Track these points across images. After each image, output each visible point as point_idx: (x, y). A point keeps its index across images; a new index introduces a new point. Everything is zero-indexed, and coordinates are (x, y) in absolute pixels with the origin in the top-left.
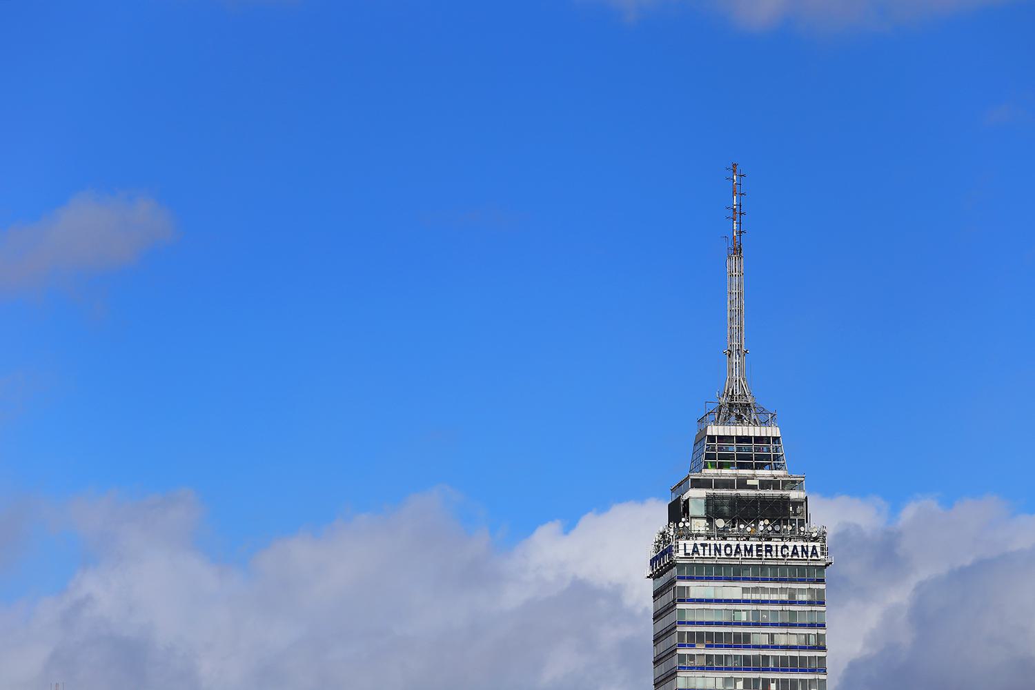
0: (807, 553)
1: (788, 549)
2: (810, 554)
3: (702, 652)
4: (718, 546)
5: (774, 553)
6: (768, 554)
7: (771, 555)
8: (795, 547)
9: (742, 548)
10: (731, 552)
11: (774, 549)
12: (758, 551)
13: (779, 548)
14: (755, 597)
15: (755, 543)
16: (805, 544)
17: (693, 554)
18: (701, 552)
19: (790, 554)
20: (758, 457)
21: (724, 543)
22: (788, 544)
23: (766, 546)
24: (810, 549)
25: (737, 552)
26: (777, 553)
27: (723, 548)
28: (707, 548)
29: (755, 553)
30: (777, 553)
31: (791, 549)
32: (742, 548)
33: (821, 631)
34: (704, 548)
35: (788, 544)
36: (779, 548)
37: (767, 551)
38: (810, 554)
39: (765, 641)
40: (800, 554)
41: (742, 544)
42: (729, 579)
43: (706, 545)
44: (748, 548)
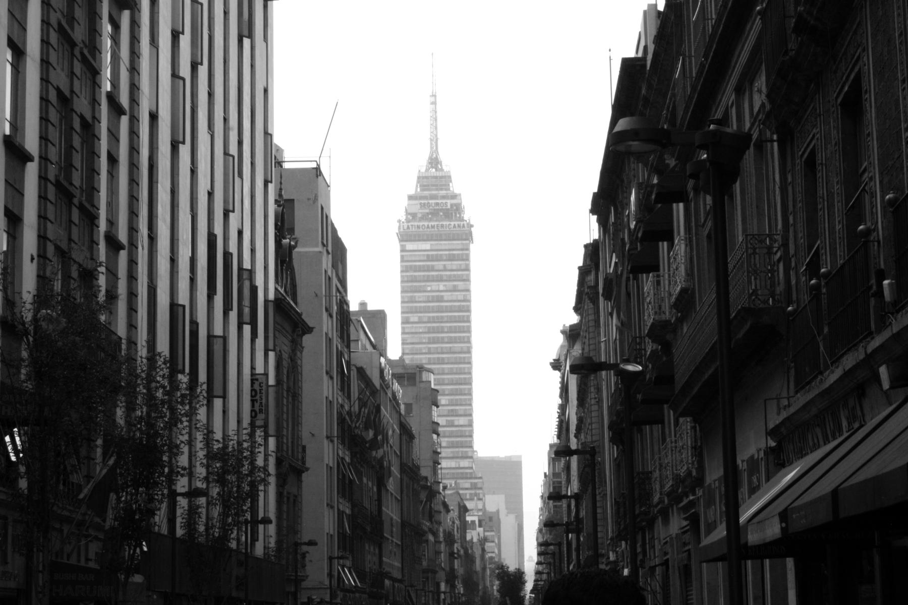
3: (412, 274)
8: (455, 225)
9: (430, 226)
14: (436, 248)
15: (436, 223)
16: (459, 223)
20: (441, 185)
21: (421, 224)
24: (462, 225)
31: (452, 226)
32: (430, 226)
33: (467, 262)
39: (441, 267)
41: (430, 224)
42: (424, 240)
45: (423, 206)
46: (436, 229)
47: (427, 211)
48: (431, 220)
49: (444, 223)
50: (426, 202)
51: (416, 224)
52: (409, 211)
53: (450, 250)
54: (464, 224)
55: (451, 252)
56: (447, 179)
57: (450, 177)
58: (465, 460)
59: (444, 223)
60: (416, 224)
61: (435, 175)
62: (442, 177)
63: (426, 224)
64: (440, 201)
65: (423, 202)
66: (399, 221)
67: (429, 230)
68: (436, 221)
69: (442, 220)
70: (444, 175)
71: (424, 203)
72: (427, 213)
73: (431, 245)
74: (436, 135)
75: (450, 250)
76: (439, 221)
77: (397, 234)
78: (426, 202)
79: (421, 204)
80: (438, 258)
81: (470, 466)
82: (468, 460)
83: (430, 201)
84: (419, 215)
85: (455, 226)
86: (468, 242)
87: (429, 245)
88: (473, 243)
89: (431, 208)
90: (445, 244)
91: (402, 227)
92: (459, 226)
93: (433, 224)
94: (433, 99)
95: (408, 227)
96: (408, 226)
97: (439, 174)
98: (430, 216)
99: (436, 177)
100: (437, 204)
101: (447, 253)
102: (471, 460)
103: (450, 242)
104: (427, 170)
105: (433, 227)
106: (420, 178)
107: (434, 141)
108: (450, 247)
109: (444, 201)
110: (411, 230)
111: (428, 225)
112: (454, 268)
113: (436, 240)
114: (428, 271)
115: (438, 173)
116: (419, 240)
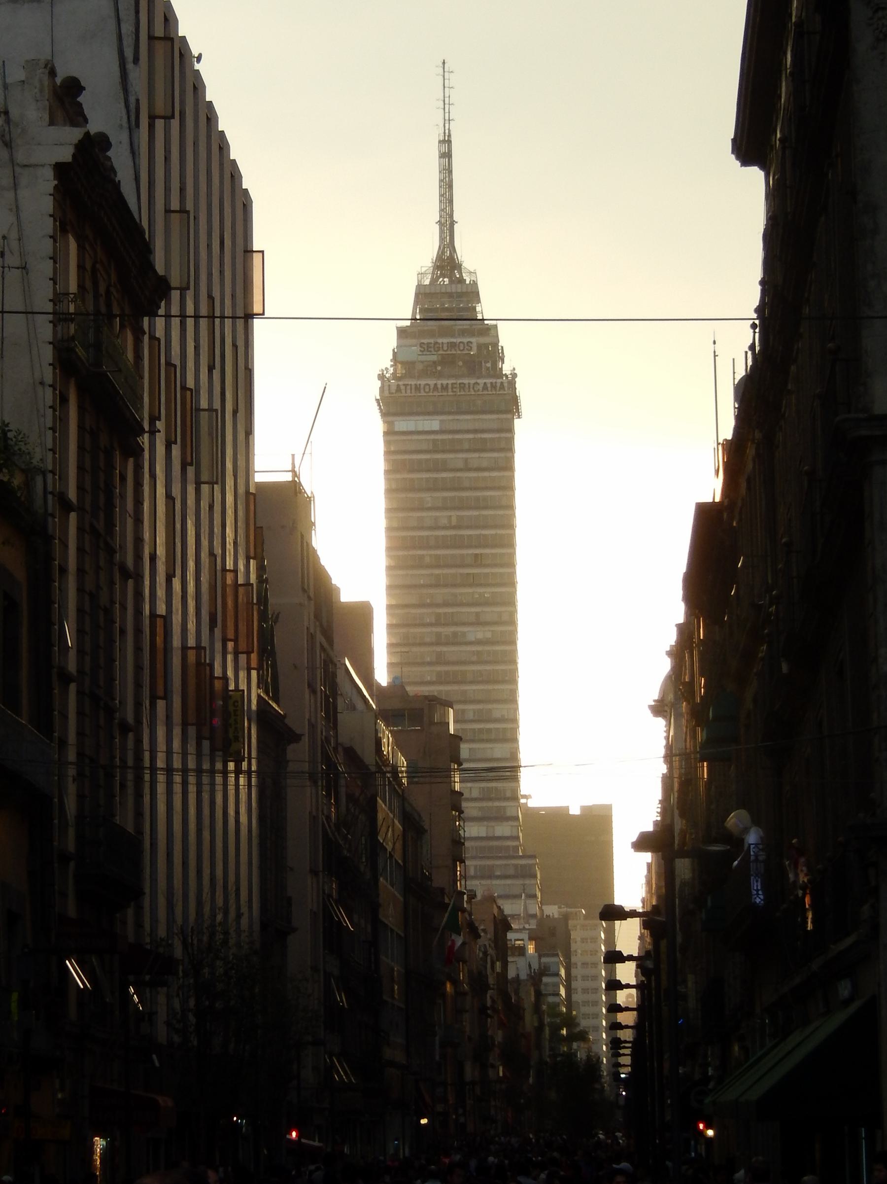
2: (498, 388)
4: (418, 386)
6: (462, 390)
9: (439, 386)
10: (430, 390)
13: (471, 386)
15: (450, 382)
16: (494, 381)
17: (396, 393)
18: (403, 391)
19: (481, 389)
21: (423, 382)
22: (479, 381)
23: (460, 384)
24: (498, 385)
25: (434, 390)
27: (422, 386)
28: (409, 387)
29: (450, 390)
31: (482, 385)
32: (439, 386)
34: (406, 388)
35: (479, 381)
38: (498, 388)
39: (460, 465)
41: (439, 382)
42: (429, 414)
43: (408, 385)
44: (444, 386)
45: (426, 348)
46: (450, 393)
47: (435, 358)
48: (440, 375)
49: (466, 381)
50: (432, 341)
51: (413, 382)
52: (400, 359)
53: (476, 431)
54: (502, 383)
55: (479, 436)
56: (472, 294)
57: (477, 294)
58: (505, 823)
59: (466, 381)
60: (413, 382)
61: (449, 290)
62: (461, 295)
63: (432, 382)
64: (458, 340)
65: (425, 341)
66: (381, 377)
67: (436, 394)
68: (450, 377)
69: (462, 376)
70: (464, 290)
71: (428, 343)
72: (434, 362)
73: (442, 421)
74: (451, 216)
75: (476, 431)
76: (456, 377)
77: (377, 400)
78: (432, 341)
79: (422, 344)
80: (454, 448)
81: (515, 834)
82: (510, 823)
83: (440, 341)
84: (420, 367)
85: (485, 387)
86: (509, 416)
87: (438, 422)
88: (519, 417)
89: (441, 352)
90: (467, 421)
91: (386, 388)
92: (494, 386)
93: (445, 382)
94: (444, 149)
95: (398, 389)
96: (398, 386)
97: (459, 288)
98: (439, 368)
99: (450, 295)
100: (452, 345)
101: (471, 436)
102: (515, 824)
103: (477, 417)
104: (433, 281)
105: (445, 388)
106: (423, 295)
107: (447, 225)
108: (477, 426)
109: (465, 340)
110: (404, 394)
111: (436, 384)
112: (485, 464)
113: (450, 413)
114: (437, 470)
115: (453, 286)
116: (418, 414)
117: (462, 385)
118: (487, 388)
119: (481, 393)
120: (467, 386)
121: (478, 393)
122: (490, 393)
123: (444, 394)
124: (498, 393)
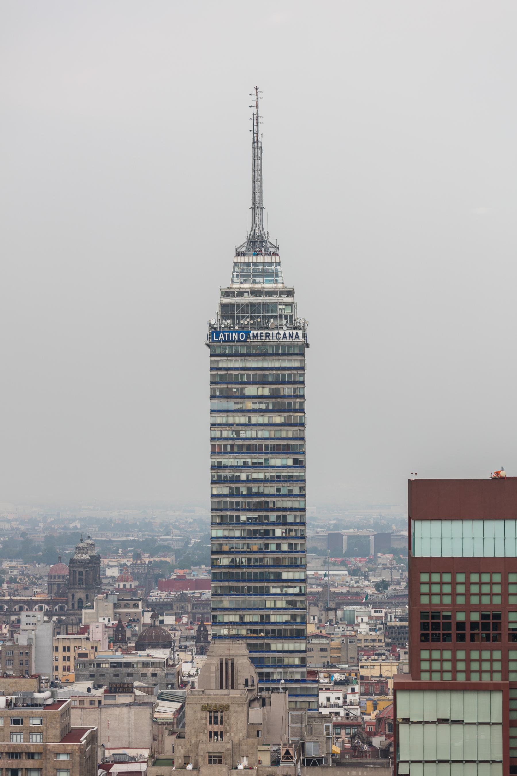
0: (292, 337)
1: (280, 334)
2: (294, 338)
5: (271, 338)
6: (267, 338)
7: (269, 339)
8: (285, 334)
11: (271, 335)
12: (261, 336)
13: (275, 335)
16: (291, 332)
22: (280, 332)
23: (266, 333)
24: (294, 335)
26: (273, 338)
29: (259, 338)
30: (273, 338)
31: (282, 335)
35: (280, 332)
36: (275, 335)
37: (266, 336)
38: (294, 338)
40: (288, 338)
54: (297, 334)
85: (285, 336)
92: (291, 336)
117: (268, 335)
118: (286, 337)
119: (282, 340)
120: (271, 335)
121: (280, 340)
122: (288, 340)
123: (255, 340)
124: (294, 340)
